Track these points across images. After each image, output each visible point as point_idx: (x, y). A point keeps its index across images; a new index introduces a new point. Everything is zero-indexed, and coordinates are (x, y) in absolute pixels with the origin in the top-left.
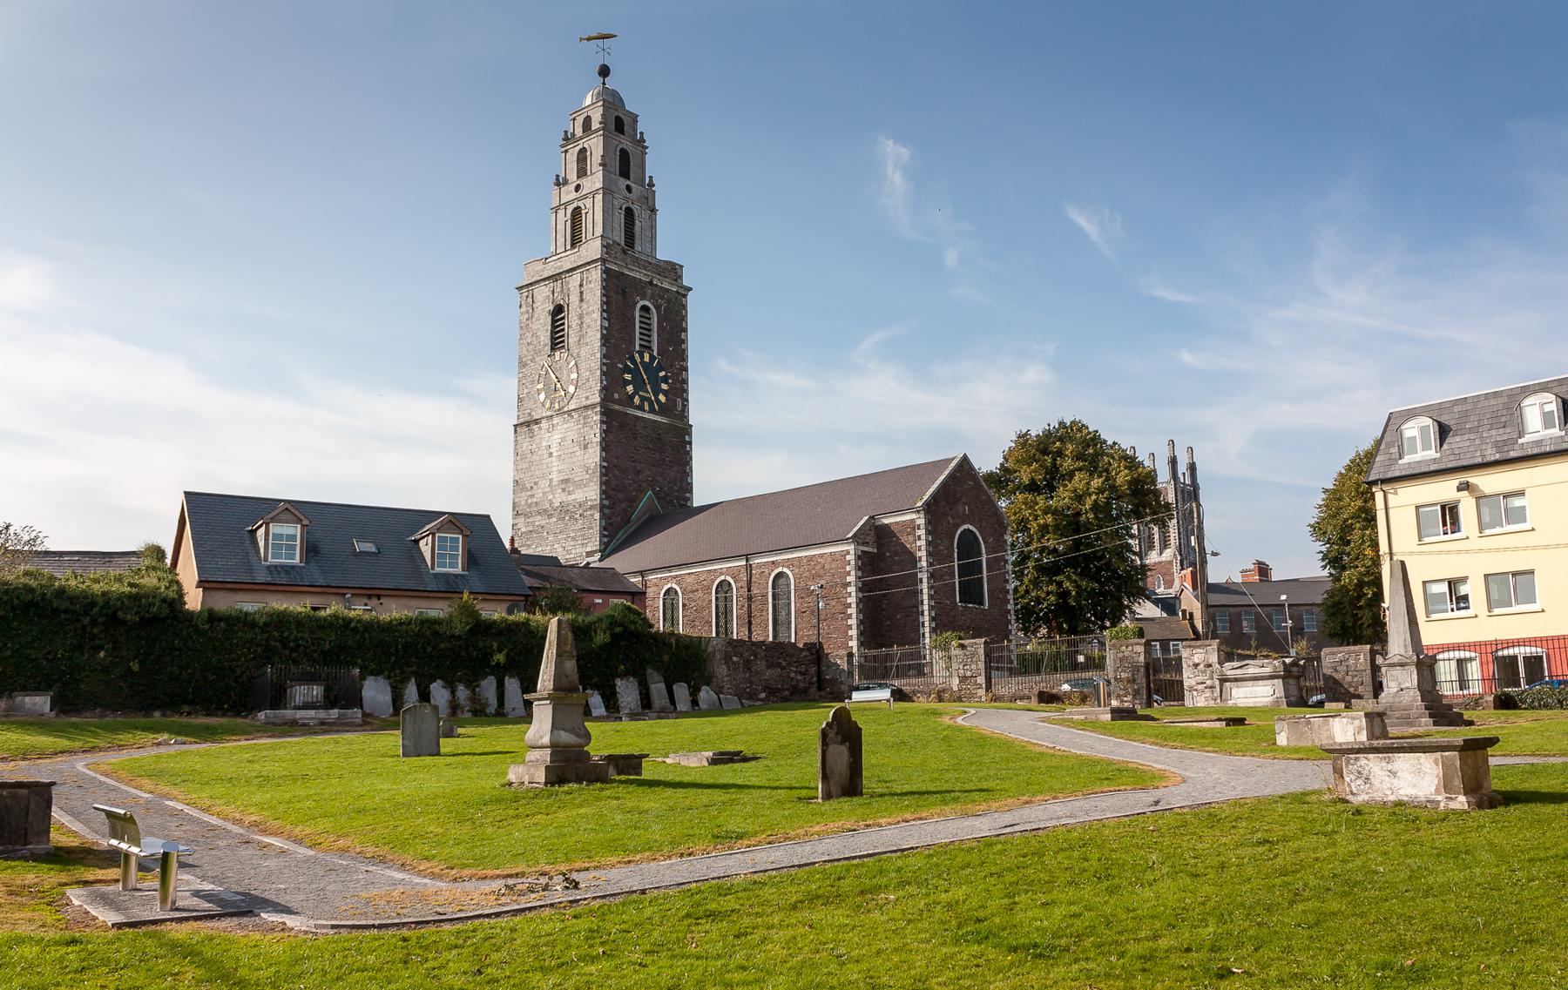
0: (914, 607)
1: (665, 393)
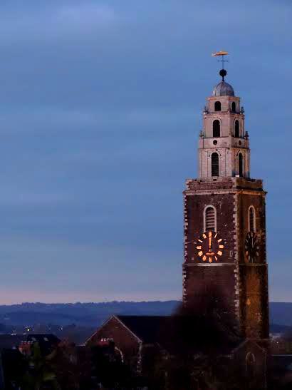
1: (221, 250)
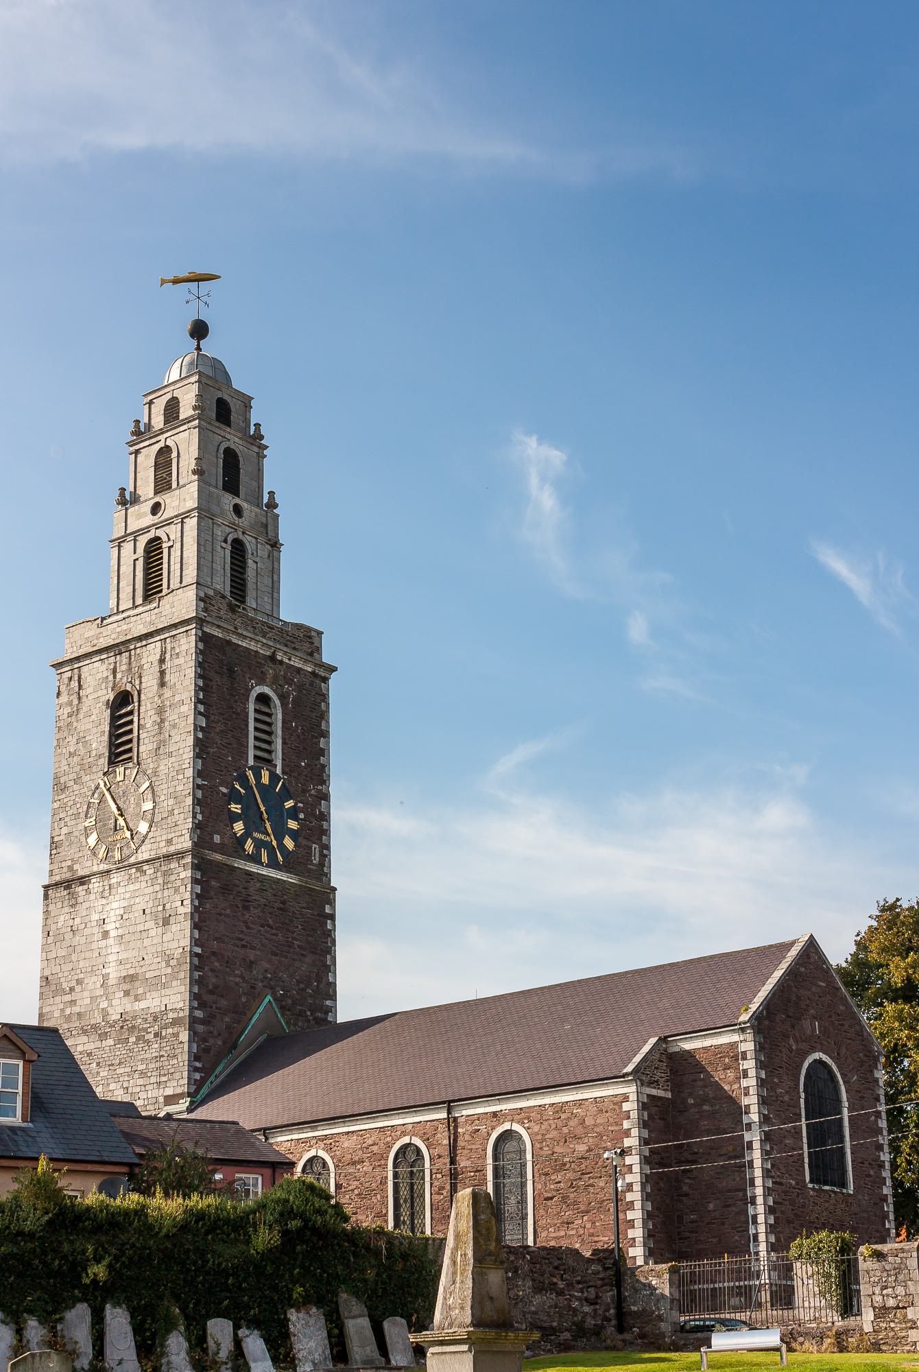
0: (739, 1190)
1: (294, 835)
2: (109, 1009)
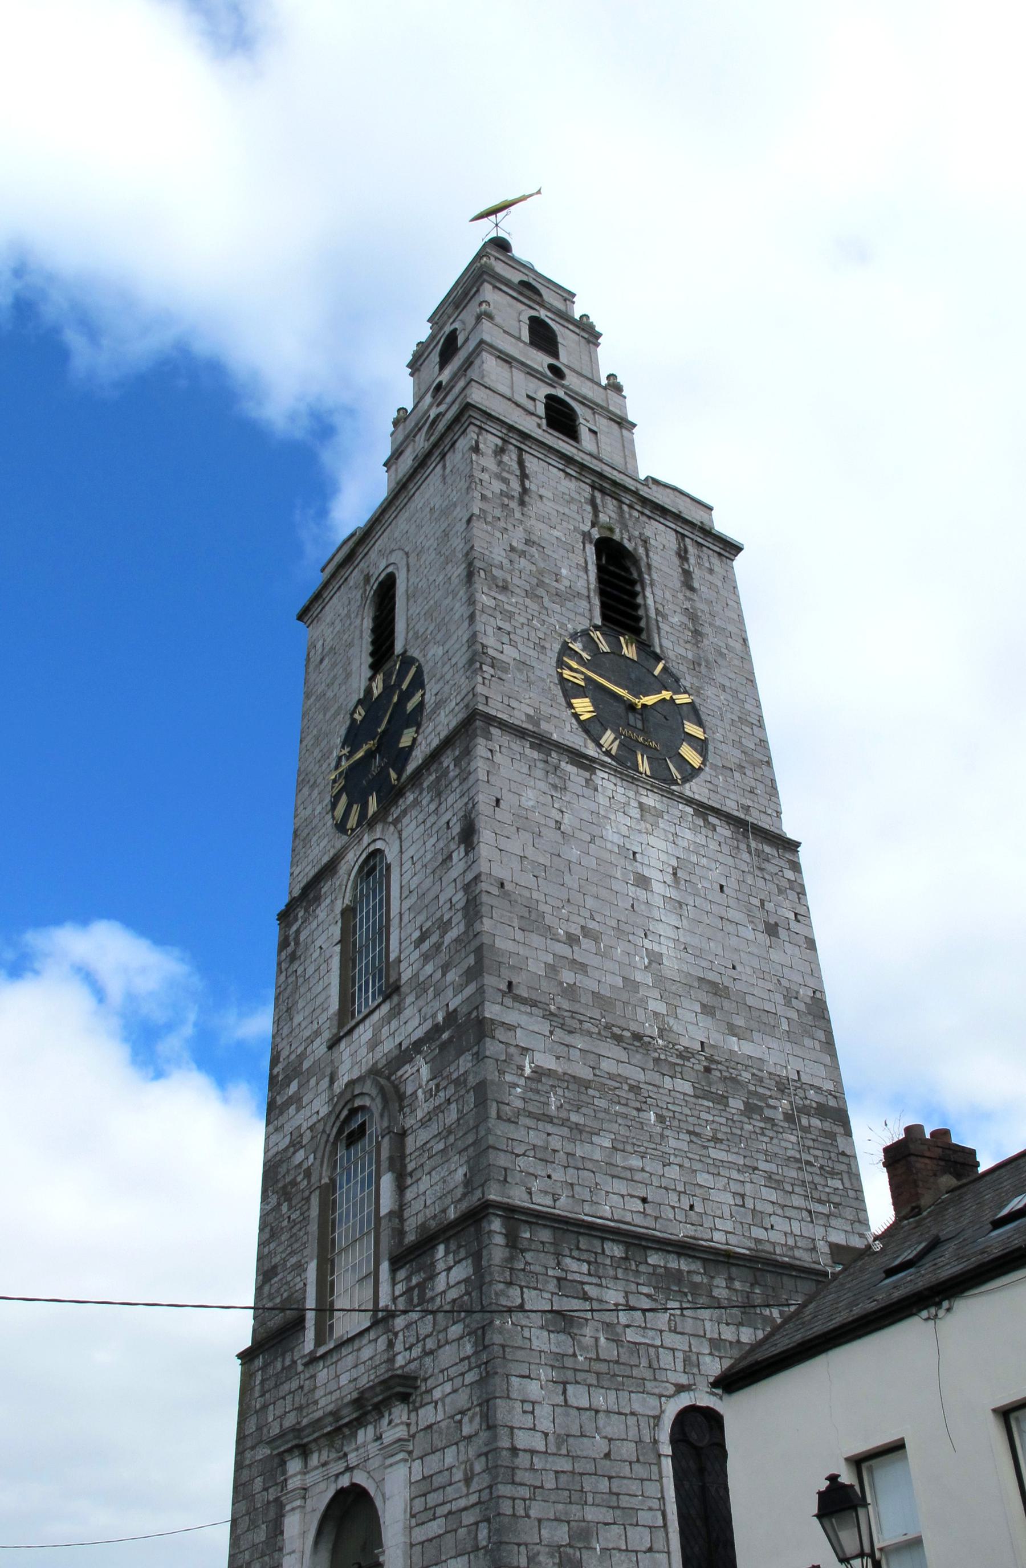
2: (672, 1021)
